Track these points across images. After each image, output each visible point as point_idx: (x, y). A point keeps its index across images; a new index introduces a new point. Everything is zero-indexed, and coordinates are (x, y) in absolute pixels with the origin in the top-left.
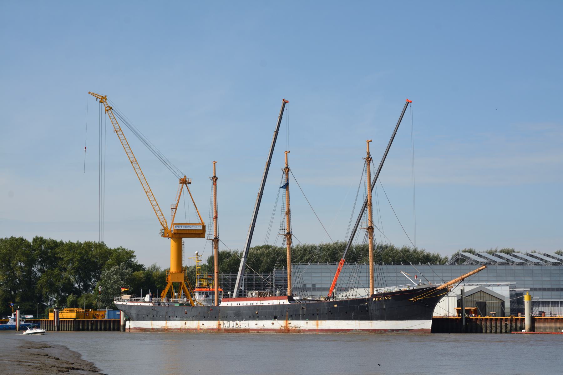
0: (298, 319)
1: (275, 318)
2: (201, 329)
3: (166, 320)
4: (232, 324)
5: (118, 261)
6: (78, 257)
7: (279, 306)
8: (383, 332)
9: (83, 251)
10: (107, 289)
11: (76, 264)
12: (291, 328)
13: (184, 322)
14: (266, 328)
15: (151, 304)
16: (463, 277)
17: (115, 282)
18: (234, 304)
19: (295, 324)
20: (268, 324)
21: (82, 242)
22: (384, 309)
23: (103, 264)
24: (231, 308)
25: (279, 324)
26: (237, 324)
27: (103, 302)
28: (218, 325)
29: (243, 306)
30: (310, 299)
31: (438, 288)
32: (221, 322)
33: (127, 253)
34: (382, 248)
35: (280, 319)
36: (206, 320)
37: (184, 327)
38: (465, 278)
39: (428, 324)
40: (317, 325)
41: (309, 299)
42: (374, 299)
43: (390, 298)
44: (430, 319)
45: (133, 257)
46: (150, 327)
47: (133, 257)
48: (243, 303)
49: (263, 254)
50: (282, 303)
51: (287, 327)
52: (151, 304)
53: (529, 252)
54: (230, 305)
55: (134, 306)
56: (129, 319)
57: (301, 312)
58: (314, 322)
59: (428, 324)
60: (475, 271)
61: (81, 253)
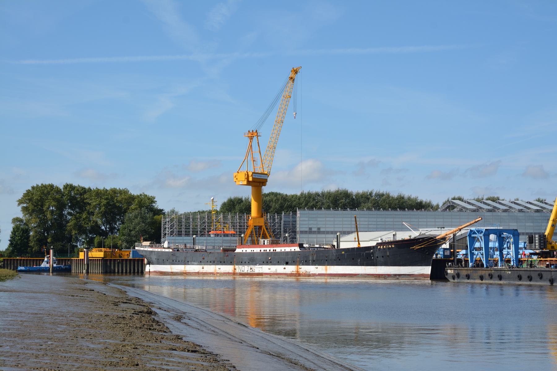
1: (287, 264)
2: (218, 273)
3: (185, 264)
4: (246, 269)
6: (104, 202)
7: (291, 252)
9: (110, 197)
10: (130, 231)
13: (201, 266)
14: (278, 272)
15: (171, 250)
16: (460, 227)
18: (249, 250)
19: (304, 269)
20: (280, 269)
21: (108, 188)
22: (388, 256)
25: (291, 269)
26: (251, 269)
31: (437, 238)
32: (237, 267)
33: (149, 199)
37: (202, 271)
39: (427, 270)
40: (326, 270)
42: (379, 247)
43: (393, 246)
45: (154, 202)
46: (170, 271)
47: (154, 202)
48: (257, 250)
50: (293, 250)
51: (298, 271)
52: (171, 250)
54: (244, 251)
57: (311, 259)
58: (323, 267)
59: (427, 270)
60: (472, 222)
61: (107, 199)
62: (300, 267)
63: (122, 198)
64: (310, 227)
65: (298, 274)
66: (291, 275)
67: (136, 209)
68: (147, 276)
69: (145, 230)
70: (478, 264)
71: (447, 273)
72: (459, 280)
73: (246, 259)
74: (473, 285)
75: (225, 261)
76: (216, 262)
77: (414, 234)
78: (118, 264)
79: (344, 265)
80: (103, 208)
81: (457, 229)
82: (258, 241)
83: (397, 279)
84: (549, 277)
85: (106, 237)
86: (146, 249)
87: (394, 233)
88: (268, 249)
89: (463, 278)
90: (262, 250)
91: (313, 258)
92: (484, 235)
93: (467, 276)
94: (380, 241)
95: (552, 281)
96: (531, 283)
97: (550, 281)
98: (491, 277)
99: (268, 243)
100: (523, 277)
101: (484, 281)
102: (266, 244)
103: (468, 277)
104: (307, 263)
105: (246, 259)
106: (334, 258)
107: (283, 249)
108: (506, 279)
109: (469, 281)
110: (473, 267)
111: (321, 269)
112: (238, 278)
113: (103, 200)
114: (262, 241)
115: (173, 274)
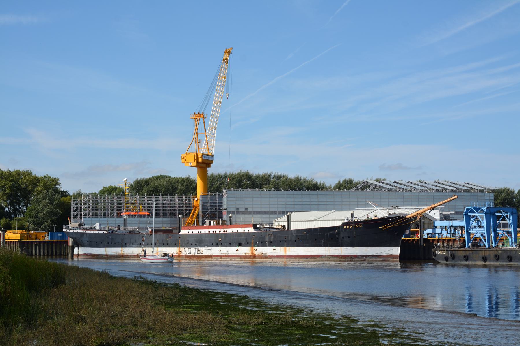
0: (264, 246)
1: (240, 245)
3: (122, 246)
4: (193, 251)
5: (47, 187)
6: (9, 184)
7: (244, 233)
8: (353, 257)
9: (14, 178)
10: (38, 212)
11: (8, 191)
12: (257, 254)
14: (230, 253)
15: (105, 232)
16: (433, 206)
17: (45, 206)
18: (196, 231)
19: (260, 250)
20: (232, 251)
23: (33, 191)
24: (193, 235)
25: (244, 251)
26: (198, 251)
27: (35, 224)
28: (178, 252)
29: (205, 234)
30: (268, 226)
31: (407, 217)
32: (182, 249)
33: (53, 181)
34: (277, 177)
35: (245, 246)
36: (165, 247)
39: (396, 251)
40: (285, 251)
41: (266, 226)
42: (345, 227)
43: (361, 226)
44: (398, 246)
45: (58, 184)
46: (104, 253)
47: (58, 184)
48: (205, 231)
49: (178, 182)
51: (252, 253)
53: (437, 180)
54: (190, 232)
55: (86, 233)
56: (78, 244)
57: (267, 239)
58: (282, 249)
59: (396, 251)
60: (446, 201)
61: (12, 181)
62: (255, 248)
63: (27, 180)
64: (246, 207)
65: (253, 256)
66: (245, 257)
67: (41, 191)
68: (75, 259)
69: (52, 212)
70: (476, 244)
72: (453, 262)
73: (192, 240)
75: (169, 242)
76: (158, 244)
77: (382, 213)
78: (36, 245)
79: (305, 246)
80: (8, 191)
81: (430, 207)
82: (204, 223)
83: (364, 260)
85: (12, 219)
86: (76, 231)
87: (352, 212)
88: (218, 231)
89: (461, 260)
90: (211, 231)
91: (270, 238)
93: (465, 257)
94: (346, 221)
98: (497, 258)
99: (215, 224)
102: (212, 225)
103: (466, 258)
104: (263, 244)
105: (192, 240)
106: (294, 239)
107: (235, 230)
109: (467, 263)
110: (469, 247)
111: (279, 251)
112: (183, 260)
113: (8, 182)
114: (208, 221)
115: (108, 257)
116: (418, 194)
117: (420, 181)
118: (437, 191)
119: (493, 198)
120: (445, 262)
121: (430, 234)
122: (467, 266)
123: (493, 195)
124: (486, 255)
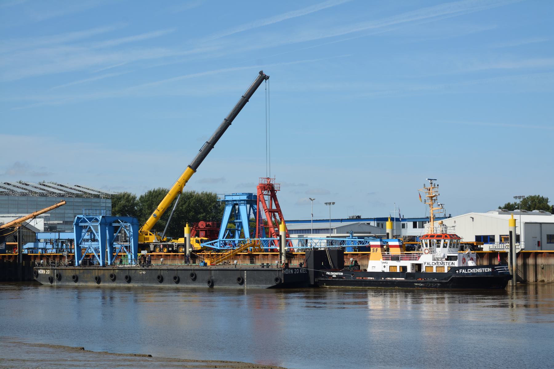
16: (35, 214)
38: (38, 215)
70: (88, 261)
71: (38, 275)
72: (60, 283)
74: (104, 289)
81: (31, 215)
84: (207, 277)
89: (69, 281)
92: (100, 224)
93: (74, 277)
95: (211, 283)
96: (179, 286)
97: (209, 282)
98: (113, 278)
100: (166, 278)
101: (101, 284)
103: (76, 279)
108: (137, 281)
109: (76, 284)
110: (79, 265)
116: (17, 198)
117: (20, 183)
118: (42, 195)
119: (110, 205)
120: (49, 284)
121: (31, 248)
122: (76, 288)
123: (110, 201)
124: (99, 275)
